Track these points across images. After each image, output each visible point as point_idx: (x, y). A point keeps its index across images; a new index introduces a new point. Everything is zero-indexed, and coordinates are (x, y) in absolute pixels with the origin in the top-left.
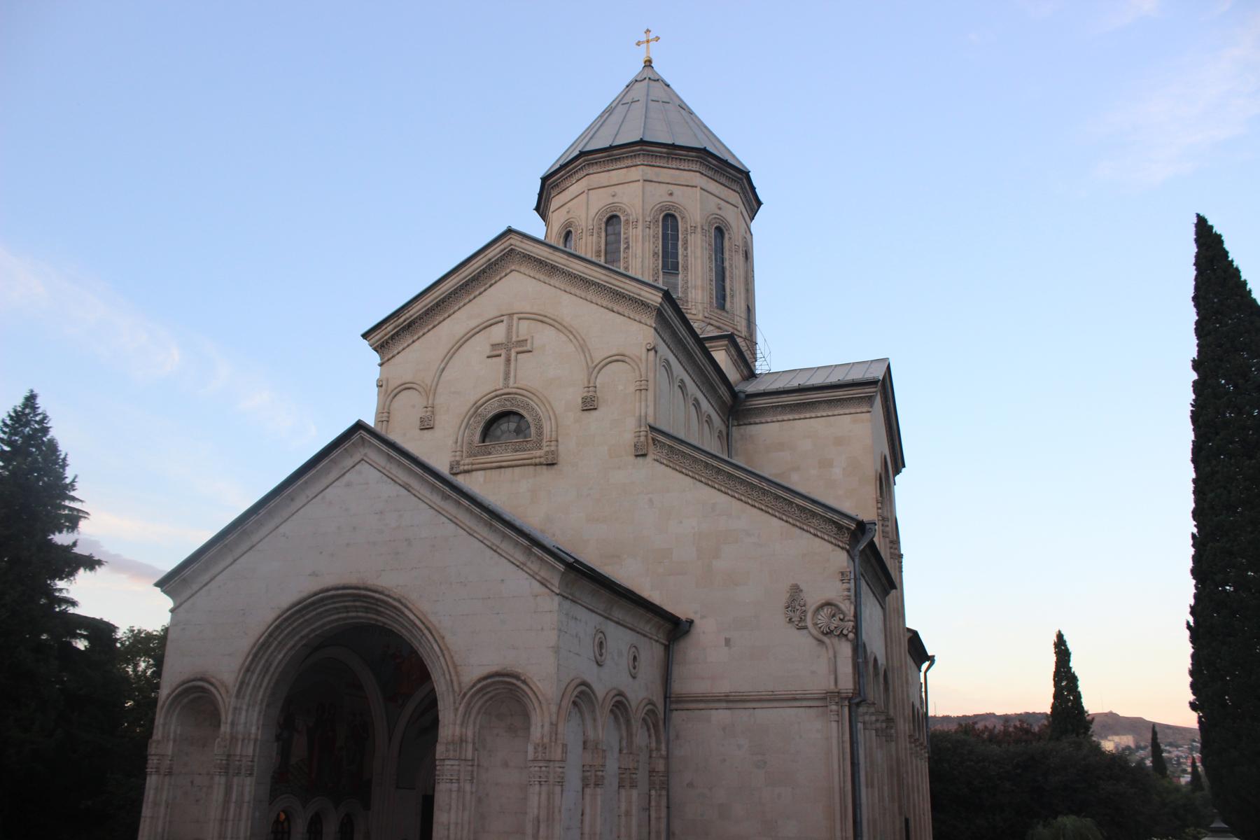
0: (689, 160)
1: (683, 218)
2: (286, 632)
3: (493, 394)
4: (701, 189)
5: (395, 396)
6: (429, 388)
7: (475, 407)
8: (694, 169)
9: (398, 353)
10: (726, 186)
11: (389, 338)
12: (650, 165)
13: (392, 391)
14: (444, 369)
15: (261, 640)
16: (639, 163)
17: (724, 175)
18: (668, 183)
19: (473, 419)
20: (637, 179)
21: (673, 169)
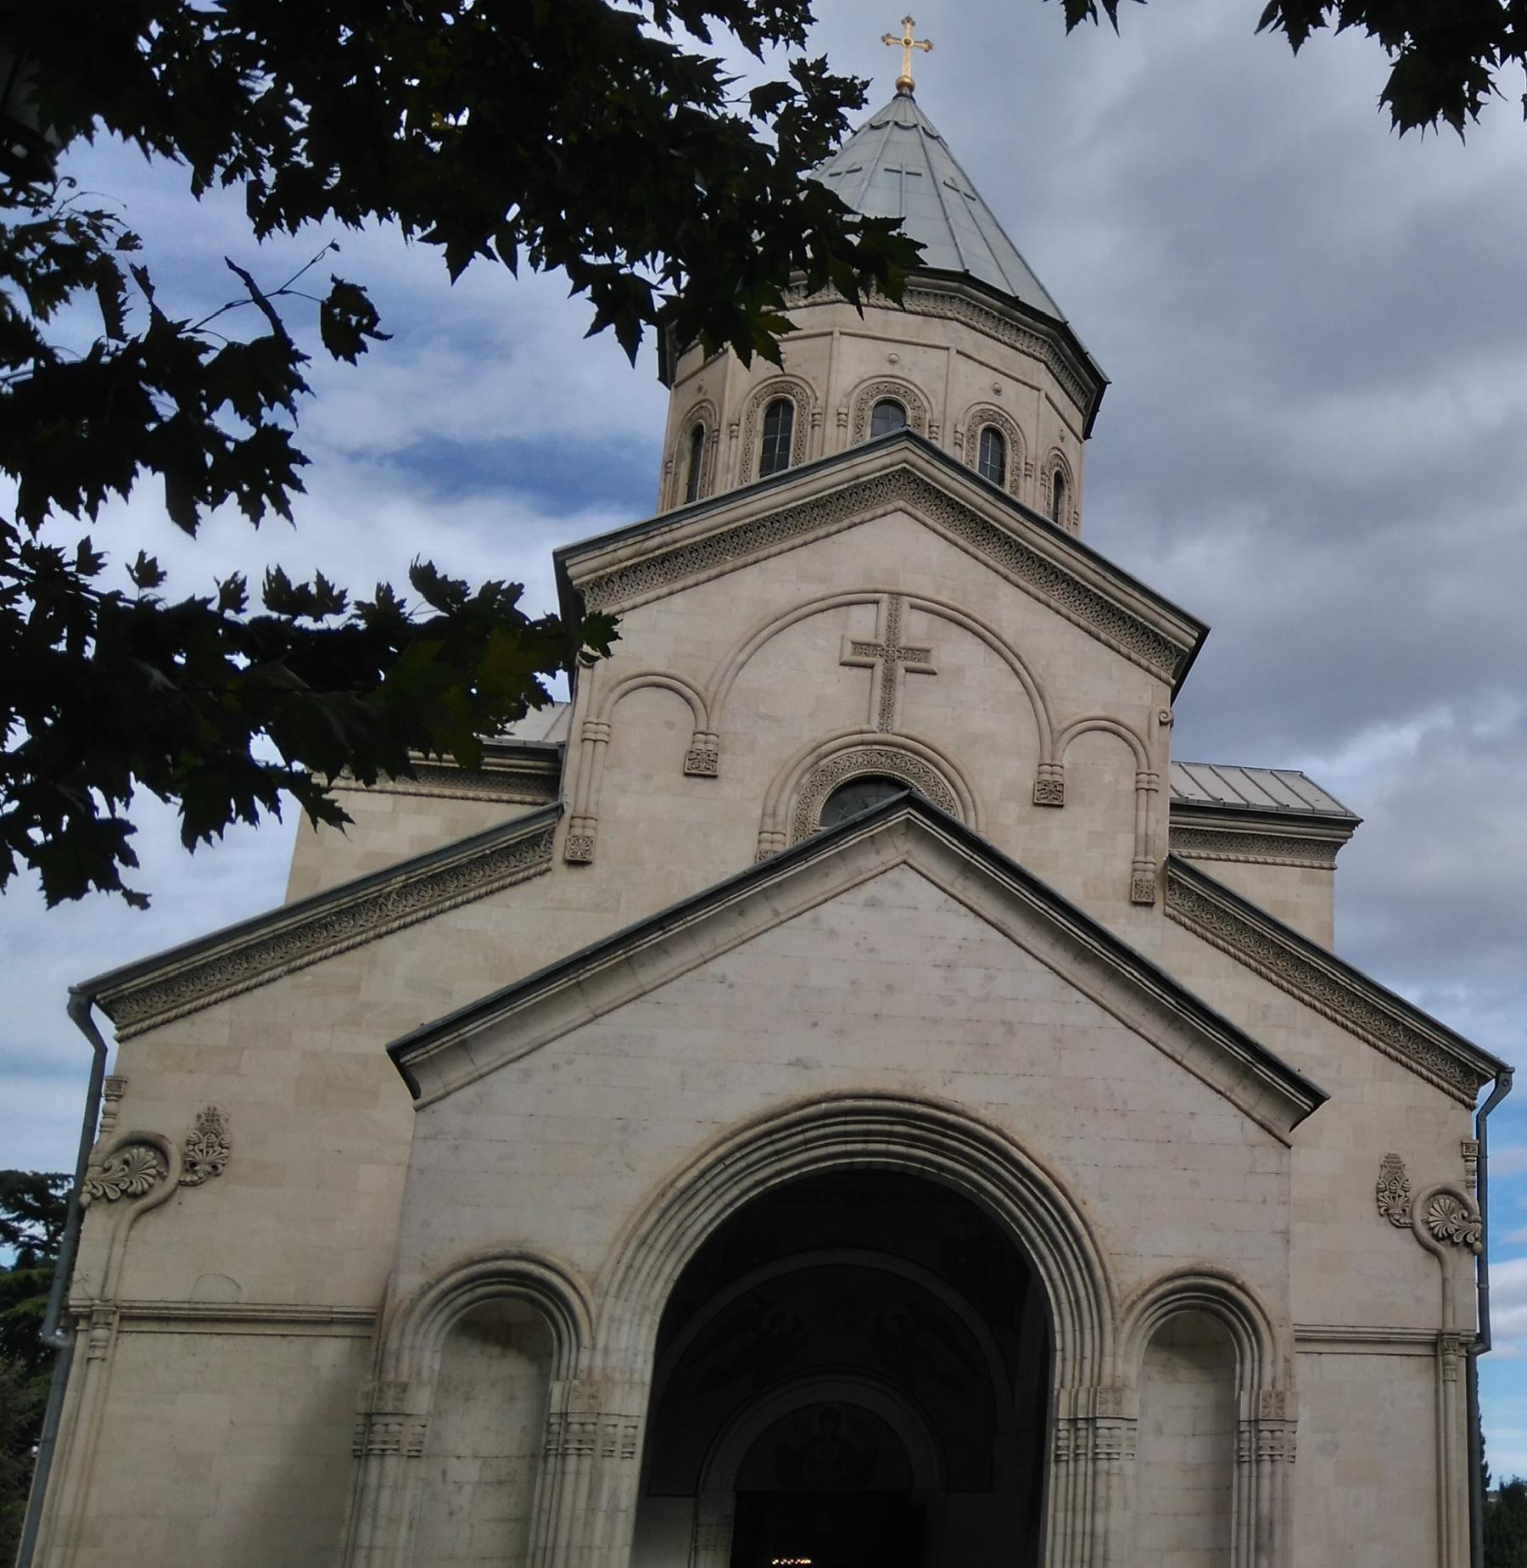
0: (1032, 335)
1: (1014, 442)
2: (732, 1170)
3: (858, 737)
4: (1047, 397)
5: (627, 693)
6: (710, 694)
7: (815, 754)
8: (1037, 354)
9: (634, 608)
10: (1072, 399)
11: (616, 572)
12: (968, 325)
13: (619, 683)
14: (743, 664)
15: (681, 1184)
16: (950, 314)
17: (1073, 377)
18: (995, 369)
19: (807, 776)
20: (944, 345)
21: (1005, 343)
